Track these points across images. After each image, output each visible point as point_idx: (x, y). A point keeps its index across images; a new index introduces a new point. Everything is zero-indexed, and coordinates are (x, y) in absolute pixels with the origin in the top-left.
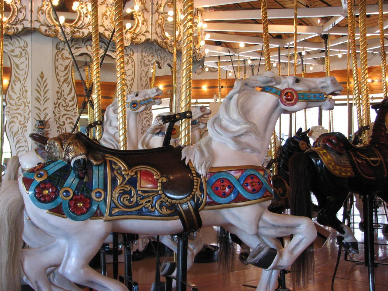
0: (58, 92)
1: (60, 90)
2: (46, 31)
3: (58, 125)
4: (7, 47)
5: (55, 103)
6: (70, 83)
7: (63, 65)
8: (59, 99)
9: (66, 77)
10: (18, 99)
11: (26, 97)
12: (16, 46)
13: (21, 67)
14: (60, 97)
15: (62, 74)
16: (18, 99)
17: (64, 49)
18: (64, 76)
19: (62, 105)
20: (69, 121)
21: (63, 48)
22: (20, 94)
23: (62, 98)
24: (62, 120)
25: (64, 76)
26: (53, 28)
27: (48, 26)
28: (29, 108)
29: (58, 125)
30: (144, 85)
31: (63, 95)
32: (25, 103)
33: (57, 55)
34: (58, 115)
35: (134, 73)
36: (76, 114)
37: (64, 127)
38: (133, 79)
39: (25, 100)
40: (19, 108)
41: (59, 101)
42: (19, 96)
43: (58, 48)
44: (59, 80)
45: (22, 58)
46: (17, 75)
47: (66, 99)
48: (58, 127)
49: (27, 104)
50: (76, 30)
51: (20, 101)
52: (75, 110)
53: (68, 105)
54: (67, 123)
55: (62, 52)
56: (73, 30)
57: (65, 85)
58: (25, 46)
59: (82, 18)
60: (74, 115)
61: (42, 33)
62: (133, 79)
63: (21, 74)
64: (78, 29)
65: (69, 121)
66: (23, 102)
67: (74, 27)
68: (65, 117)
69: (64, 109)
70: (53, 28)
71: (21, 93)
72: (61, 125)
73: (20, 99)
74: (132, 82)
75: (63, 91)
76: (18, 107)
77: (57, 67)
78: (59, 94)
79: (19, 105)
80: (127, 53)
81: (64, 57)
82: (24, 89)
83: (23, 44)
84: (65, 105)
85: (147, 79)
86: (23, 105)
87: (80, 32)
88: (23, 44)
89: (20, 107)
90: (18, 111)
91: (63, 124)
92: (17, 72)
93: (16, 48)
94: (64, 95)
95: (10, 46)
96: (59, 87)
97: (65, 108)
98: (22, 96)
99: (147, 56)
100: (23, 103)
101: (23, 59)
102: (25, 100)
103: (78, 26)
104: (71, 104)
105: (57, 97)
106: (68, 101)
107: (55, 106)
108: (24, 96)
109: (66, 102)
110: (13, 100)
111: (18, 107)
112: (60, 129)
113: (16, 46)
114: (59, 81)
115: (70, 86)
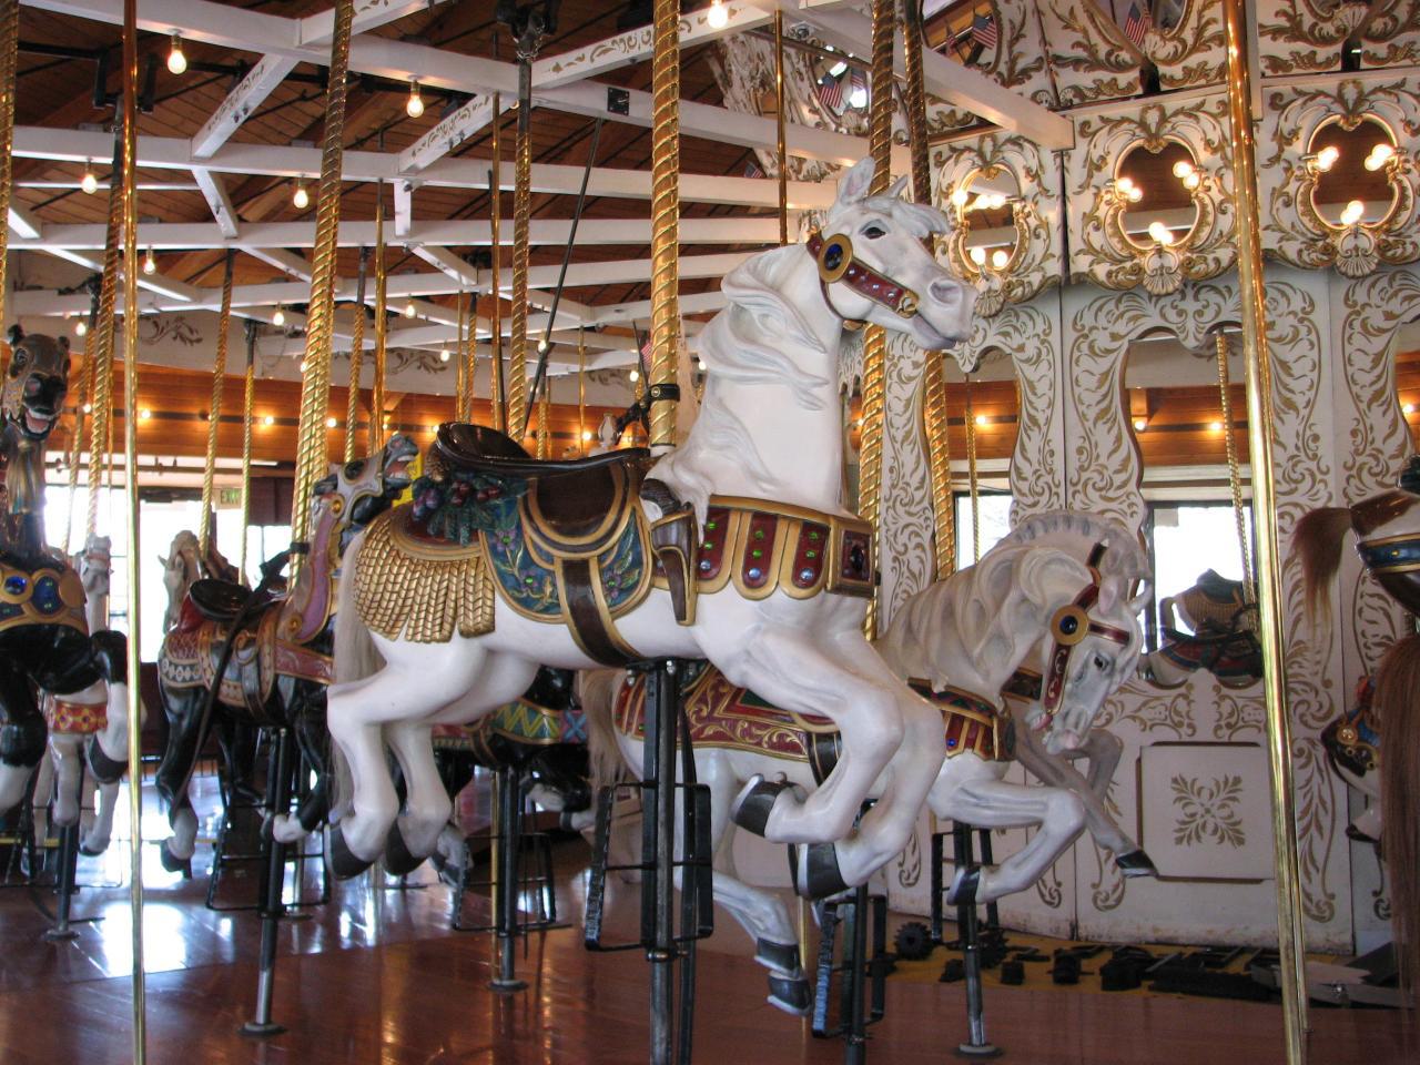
0: (1354, 433)
1: (1361, 427)
2: (1109, 274)
3: (894, 554)
5: (1350, 464)
6: (1389, 404)
7: (1366, 353)
8: (1082, 469)
9: (1104, 404)
10: (1290, 463)
11: (1315, 456)
12: (1279, 312)
13: (1297, 369)
14: (1086, 465)
15: (899, 422)
16: (1290, 463)
17: (1096, 328)
18: (1099, 403)
19: (1371, 468)
20: (916, 540)
21: (1094, 324)
22: (1297, 448)
23: (1369, 448)
24: (902, 539)
25: (1372, 384)
26: (1128, 265)
27: (1115, 261)
28: (1326, 485)
30: (899, 438)
31: (1370, 439)
32: (1312, 475)
33: (1348, 323)
34: (893, 528)
35: (1317, 366)
36: (1135, 508)
37: (905, 558)
38: (1314, 386)
39: (1313, 465)
40: (1296, 489)
41: (1360, 460)
42: (1296, 453)
43: (1079, 327)
44: (1084, 415)
45: (1300, 344)
46: (1032, 412)
47: (908, 484)
48: (895, 559)
49: (1319, 477)
50: (1391, 239)
51: (1300, 468)
52: (1132, 497)
53: (1112, 485)
54: (911, 546)
55: (1364, 315)
56: (1189, 258)
57: (1377, 410)
58: (1308, 309)
59: (1210, 219)
60: (1129, 512)
61: (1101, 284)
62: (1314, 386)
63: (1297, 390)
64: (1201, 251)
65: (916, 540)
66: (1308, 469)
67: (1388, 232)
68: (907, 532)
69: (1101, 497)
70: (1128, 265)
71: (1300, 444)
72: (898, 552)
73: (1300, 461)
74: (1048, 412)
75: (1372, 428)
76: (1293, 486)
77: (1349, 359)
78: (1359, 439)
79: (1296, 482)
80: (1291, 309)
81: (1097, 351)
82: (1308, 433)
83: (1044, 327)
84: (1101, 485)
85: (909, 420)
86: (1308, 480)
87: (1205, 259)
88: (1044, 327)
89: (1299, 486)
90: (1295, 498)
91: (902, 549)
92: (1031, 403)
93: (1280, 316)
94: (1098, 456)
95: (1016, 336)
96: (1358, 416)
97: (1379, 478)
98: (1302, 454)
99: (1379, 303)
100: (1306, 473)
101: (1303, 347)
102: (1313, 465)
103: (1397, 227)
104: (1119, 478)
105: (889, 484)
106: (1110, 472)
107: (1347, 473)
108: (1310, 453)
109: (1106, 476)
110: (1025, 479)
111: (1293, 486)
113: (1279, 312)
114: (1356, 399)
115: (1115, 431)
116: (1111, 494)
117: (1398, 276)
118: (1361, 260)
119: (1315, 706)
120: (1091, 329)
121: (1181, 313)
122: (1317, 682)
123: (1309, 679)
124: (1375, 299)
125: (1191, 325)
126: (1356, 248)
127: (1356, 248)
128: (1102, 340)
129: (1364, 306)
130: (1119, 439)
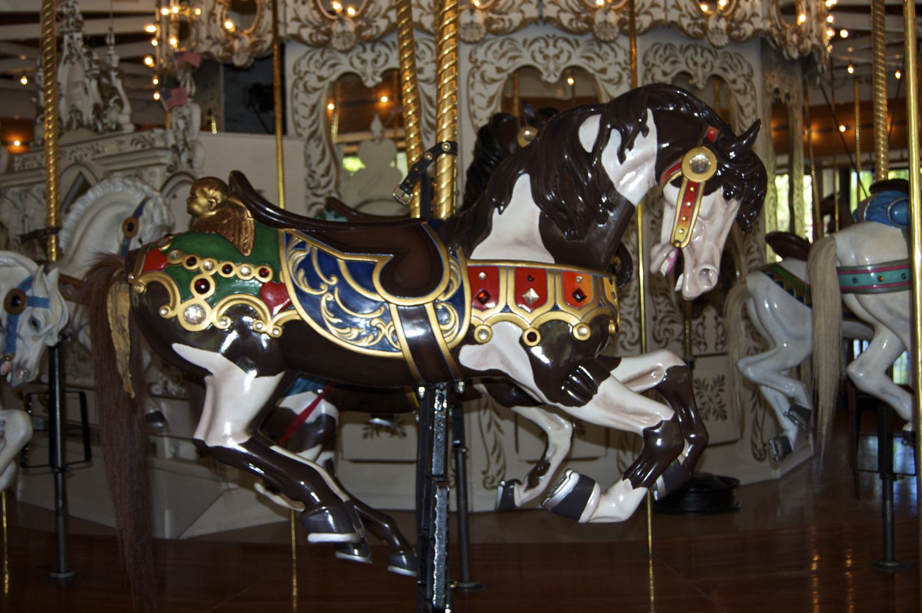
3: (652, 218)
4: (592, 64)
29: (652, 218)
72: (655, 216)
112: (654, 226)
116: (320, 192)
117: (507, 42)
118: (475, 31)
119: (629, 335)
120: (483, 62)
121: (363, 62)
122: (631, 318)
123: (627, 317)
124: (490, 57)
125: (369, 70)
126: (472, 23)
127: (472, 23)
128: (490, 72)
129: (483, 62)
130: (323, 153)
